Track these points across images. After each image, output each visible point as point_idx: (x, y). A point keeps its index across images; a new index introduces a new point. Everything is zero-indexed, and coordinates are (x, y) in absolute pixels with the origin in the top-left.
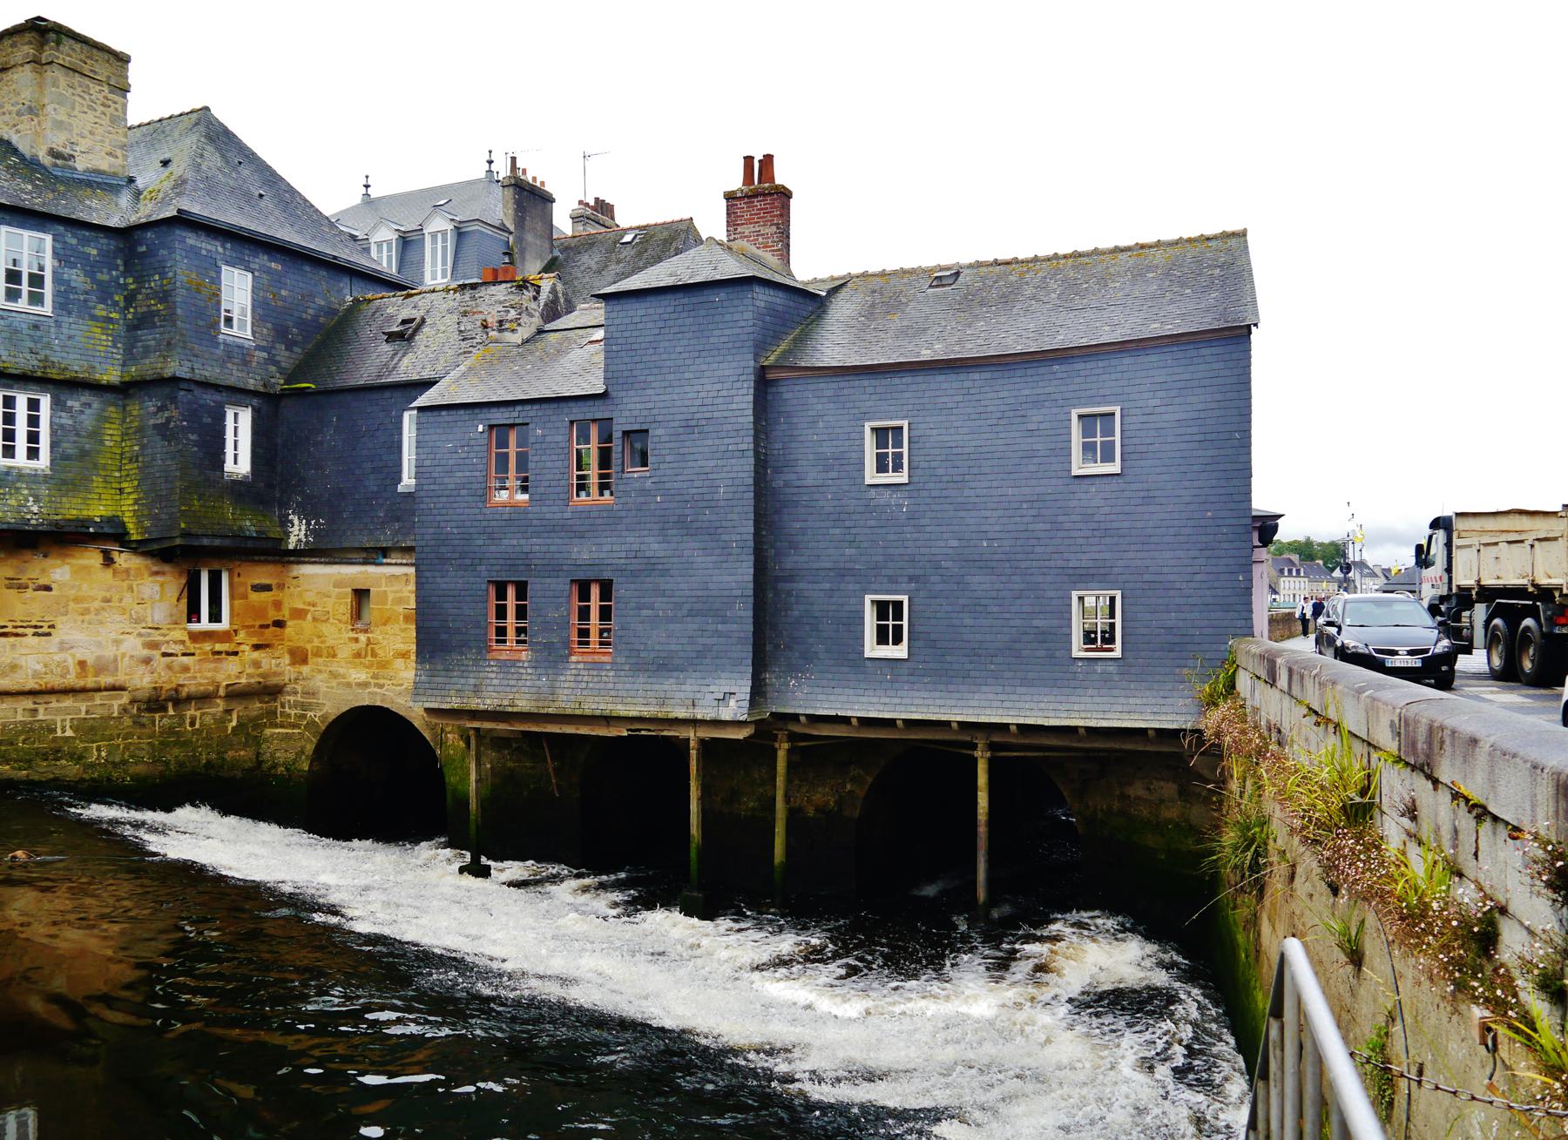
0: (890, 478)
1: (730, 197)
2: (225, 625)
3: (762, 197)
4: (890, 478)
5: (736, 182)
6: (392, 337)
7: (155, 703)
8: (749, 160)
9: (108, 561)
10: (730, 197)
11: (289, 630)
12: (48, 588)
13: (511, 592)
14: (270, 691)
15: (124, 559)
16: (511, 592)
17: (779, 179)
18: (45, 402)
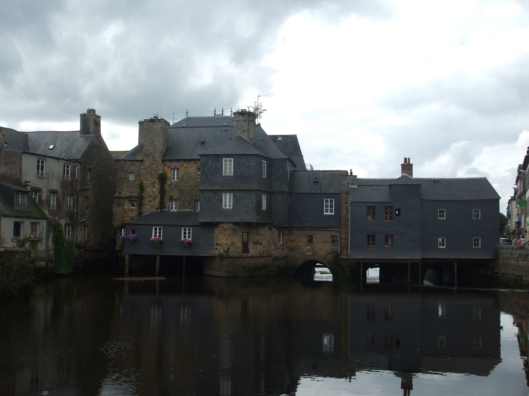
0: (441, 218)
1: (402, 165)
2: (281, 243)
3: (407, 167)
4: (441, 218)
5: (403, 162)
6: (314, 182)
7: (277, 259)
8: (405, 159)
9: (270, 229)
10: (402, 165)
11: (289, 244)
12: (261, 235)
13: (371, 237)
14: (285, 258)
15: (274, 229)
16: (371, 237)
17: (411, 163)
18: (265, 196)
